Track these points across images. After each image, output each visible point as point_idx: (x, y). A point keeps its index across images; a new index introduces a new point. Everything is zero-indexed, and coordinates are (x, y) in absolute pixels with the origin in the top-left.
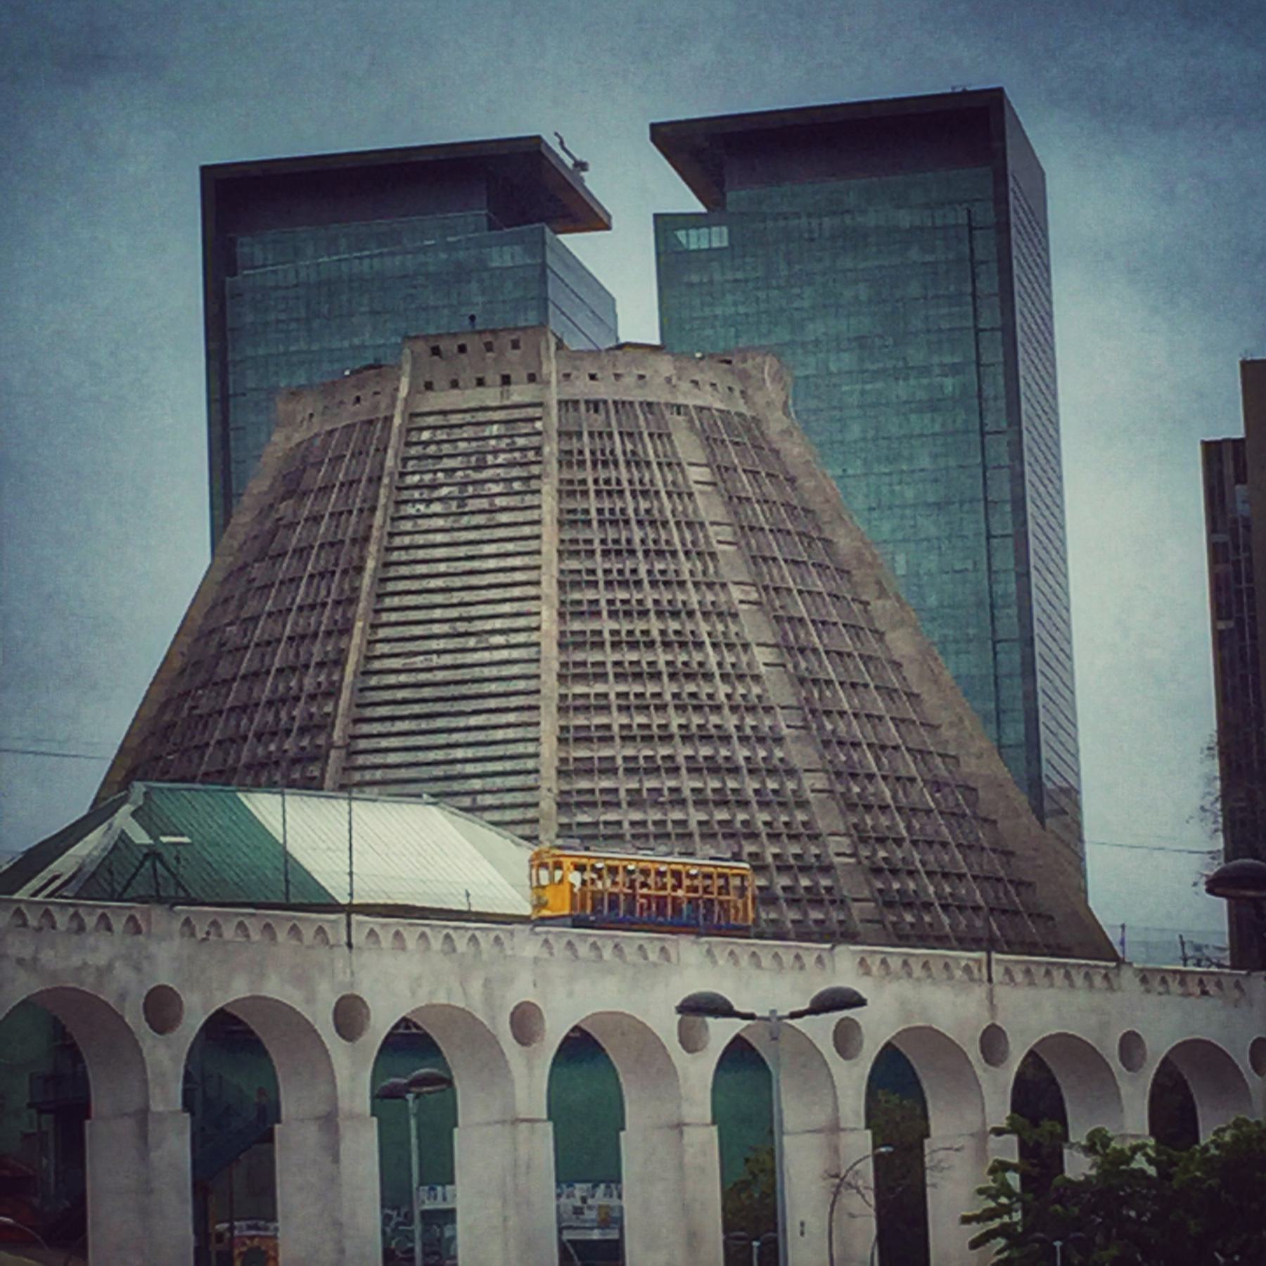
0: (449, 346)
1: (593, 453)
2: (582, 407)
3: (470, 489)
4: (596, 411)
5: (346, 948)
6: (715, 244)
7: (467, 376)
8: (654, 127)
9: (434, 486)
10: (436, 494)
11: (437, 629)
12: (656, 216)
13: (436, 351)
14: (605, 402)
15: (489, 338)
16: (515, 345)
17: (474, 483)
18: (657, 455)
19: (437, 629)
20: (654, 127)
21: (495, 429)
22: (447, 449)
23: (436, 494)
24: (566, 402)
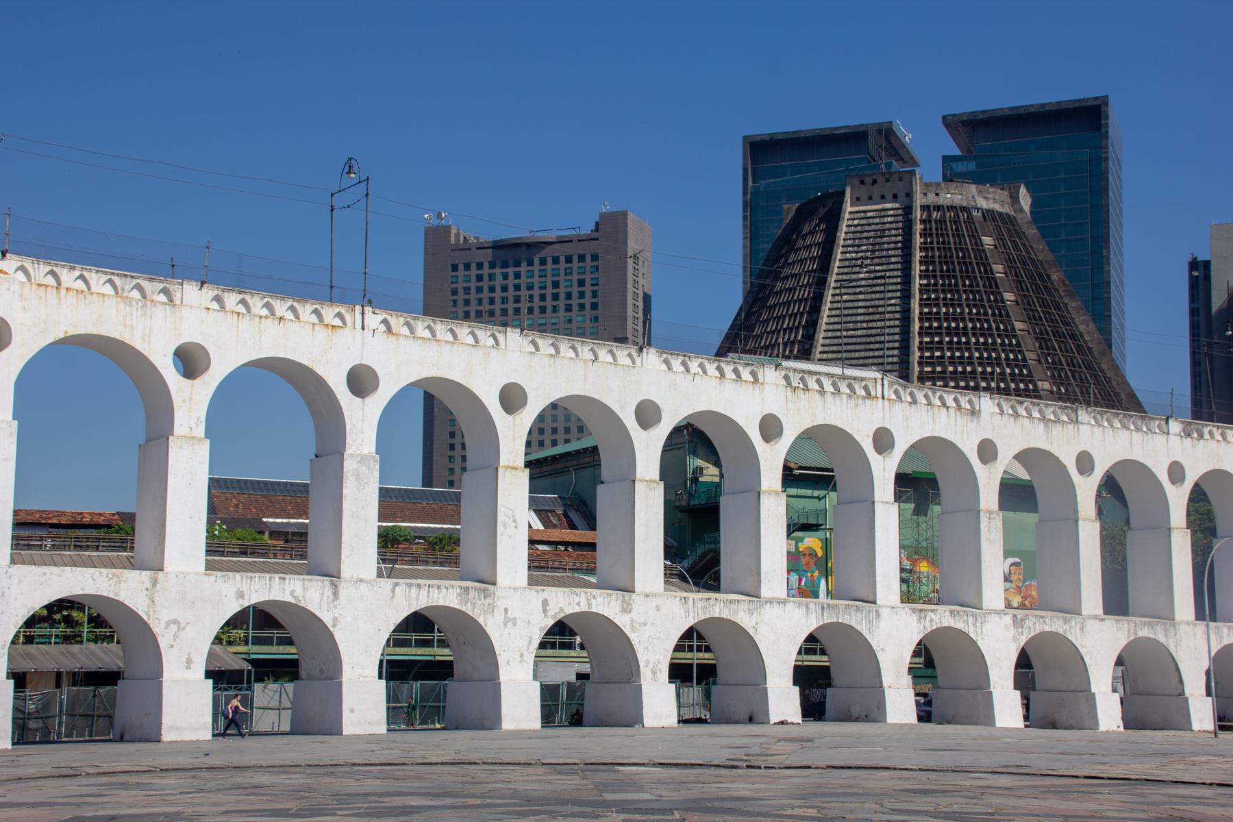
0: (868, 180)
1: (937, 229)
2: (932, 209)
3: (877, 247)
4: (938, 211)
5: (880, 400)
6: (970, 169)
7: (876, 196)
8: (944, 118)
9: (859, 246)
10: (860, 249)
11: (860, 311)
12: (944, 158)
13: (862, 182)
14: (943, 206)
15: (887, 176)
16: (900, 179)
17: (879, 244)
18: (968, 232)
19: (860, 311)
20: (944, 118)
21: (890, 219)
22: (867, 228)
23: (860, 249)
24: (924, 206)
